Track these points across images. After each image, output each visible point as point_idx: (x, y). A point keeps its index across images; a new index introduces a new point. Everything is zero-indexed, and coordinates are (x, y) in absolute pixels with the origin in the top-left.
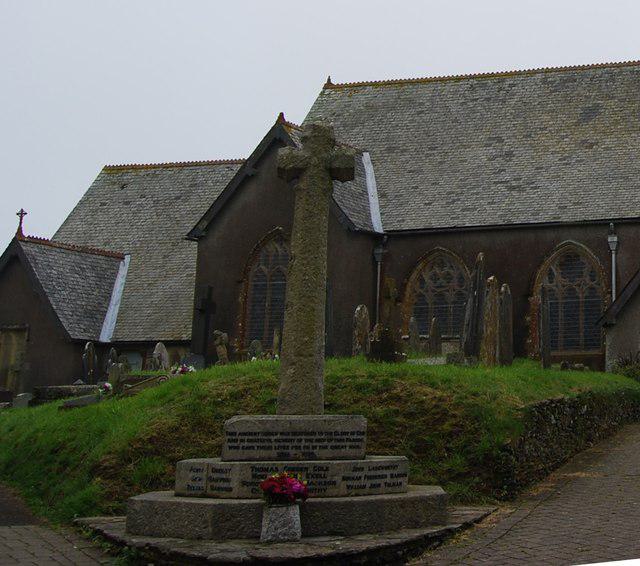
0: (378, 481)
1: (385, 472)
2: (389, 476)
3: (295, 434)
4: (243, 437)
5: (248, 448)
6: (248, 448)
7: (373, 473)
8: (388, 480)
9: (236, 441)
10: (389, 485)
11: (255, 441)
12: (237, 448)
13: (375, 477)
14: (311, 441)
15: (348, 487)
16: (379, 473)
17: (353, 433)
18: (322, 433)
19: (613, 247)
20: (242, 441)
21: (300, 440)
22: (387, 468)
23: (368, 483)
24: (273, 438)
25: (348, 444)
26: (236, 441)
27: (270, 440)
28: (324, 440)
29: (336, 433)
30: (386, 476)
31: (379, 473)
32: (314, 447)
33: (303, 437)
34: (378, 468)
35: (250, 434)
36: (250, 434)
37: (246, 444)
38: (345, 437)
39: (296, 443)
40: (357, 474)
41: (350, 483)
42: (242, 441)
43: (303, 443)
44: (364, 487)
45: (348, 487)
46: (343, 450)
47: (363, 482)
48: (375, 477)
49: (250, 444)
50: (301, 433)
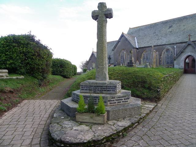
0: (120, 101)
1: (122, 98)
2: (123, 99)
3: (97, 86)
4: (85, 87)
5: (86, 90)
6: (86, 90)
7: (118, 99)
8: (123, 100)
9: (83, 88)
10: (124, 102)
11: (88, 88)
12: (83, 90)
13: (119, 100)
14: (102, 88)
15: (110, 103)
16: (120, 99)
17: (113, 87)
18: (104, 87)
19: (175, 47)
20: (85, 88)
21: (99, 88)
22: (123, 97)
23: (117, 102)
24: (92, 87)
25: (112, 90)
26: (83, 88)
27: (91, 88)
28: (105, 88)
29: (108, 87)
30: (122, 99)
31: (120, 99)
32: (103, 90)
33: (100, 87)
34: (119, 97)
35: (86, 86)
36: (86, 86)
37: (85, 89)
38: (111, 88)
39: (98, 89)
40: (112, 99)
41: (111, 102)
42: (85, 88)
43: (100, 89)
44: (116, 103)
45: (110, 103)
46: (110, 91)
47: (115, 102)
48: (119, 100)
49: (87, 89)
50: (99, 86)
